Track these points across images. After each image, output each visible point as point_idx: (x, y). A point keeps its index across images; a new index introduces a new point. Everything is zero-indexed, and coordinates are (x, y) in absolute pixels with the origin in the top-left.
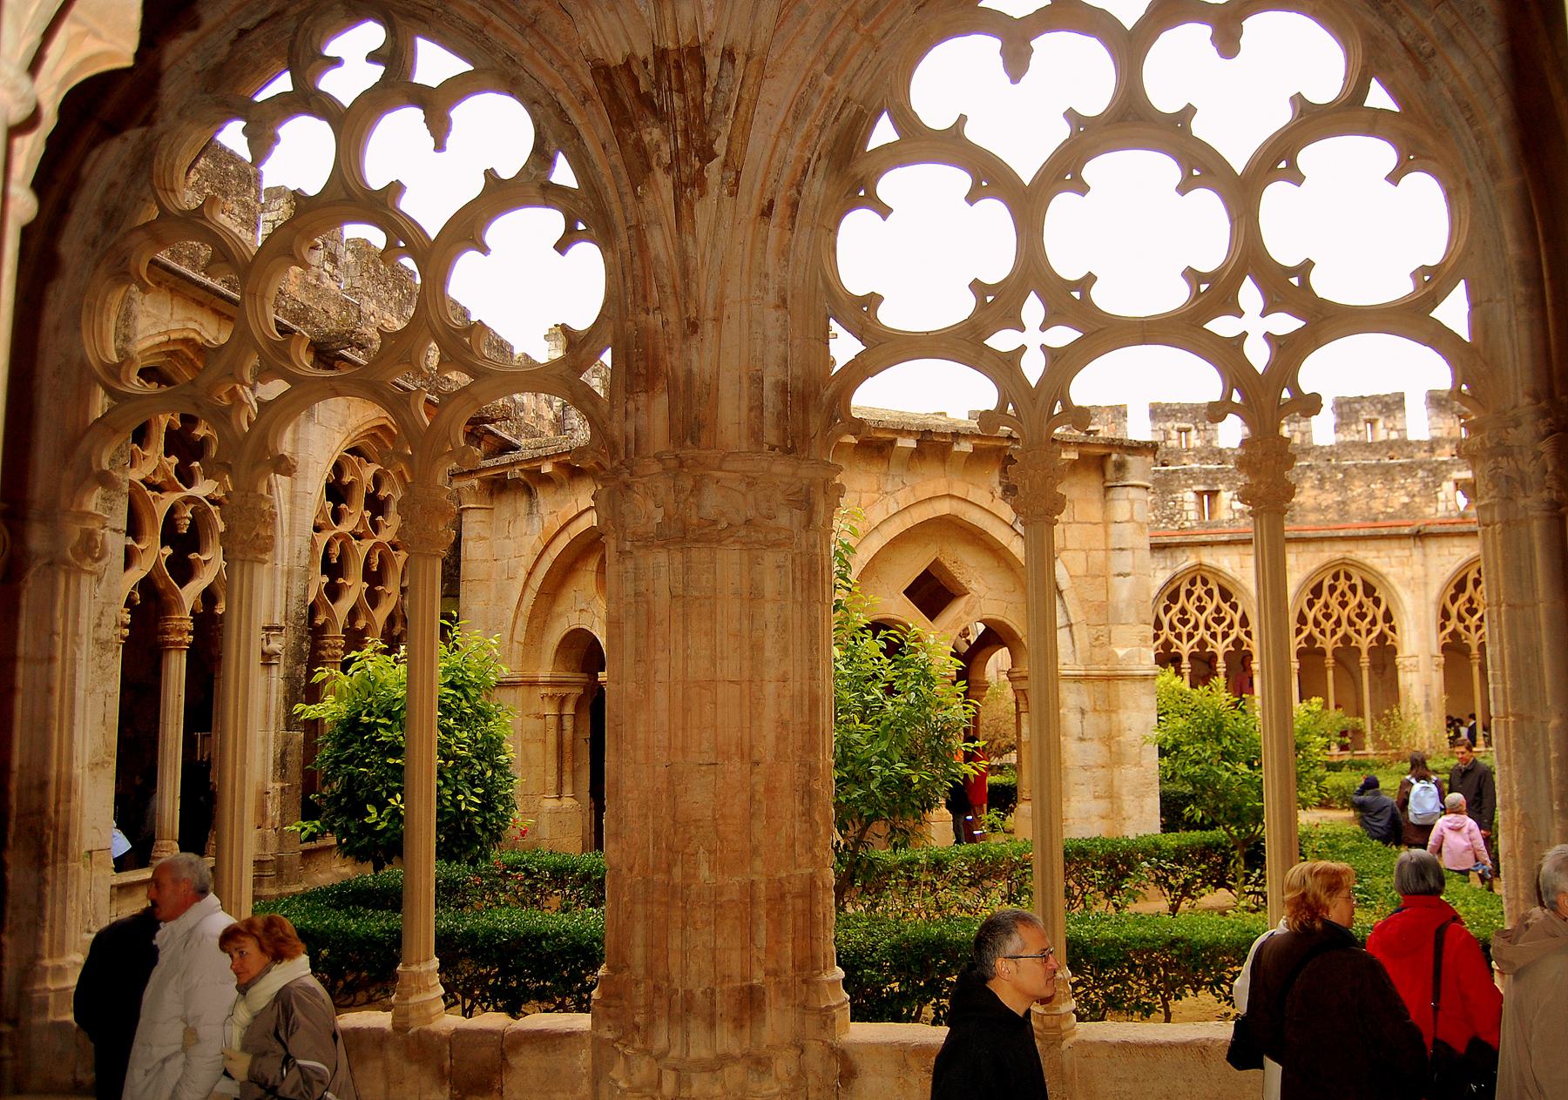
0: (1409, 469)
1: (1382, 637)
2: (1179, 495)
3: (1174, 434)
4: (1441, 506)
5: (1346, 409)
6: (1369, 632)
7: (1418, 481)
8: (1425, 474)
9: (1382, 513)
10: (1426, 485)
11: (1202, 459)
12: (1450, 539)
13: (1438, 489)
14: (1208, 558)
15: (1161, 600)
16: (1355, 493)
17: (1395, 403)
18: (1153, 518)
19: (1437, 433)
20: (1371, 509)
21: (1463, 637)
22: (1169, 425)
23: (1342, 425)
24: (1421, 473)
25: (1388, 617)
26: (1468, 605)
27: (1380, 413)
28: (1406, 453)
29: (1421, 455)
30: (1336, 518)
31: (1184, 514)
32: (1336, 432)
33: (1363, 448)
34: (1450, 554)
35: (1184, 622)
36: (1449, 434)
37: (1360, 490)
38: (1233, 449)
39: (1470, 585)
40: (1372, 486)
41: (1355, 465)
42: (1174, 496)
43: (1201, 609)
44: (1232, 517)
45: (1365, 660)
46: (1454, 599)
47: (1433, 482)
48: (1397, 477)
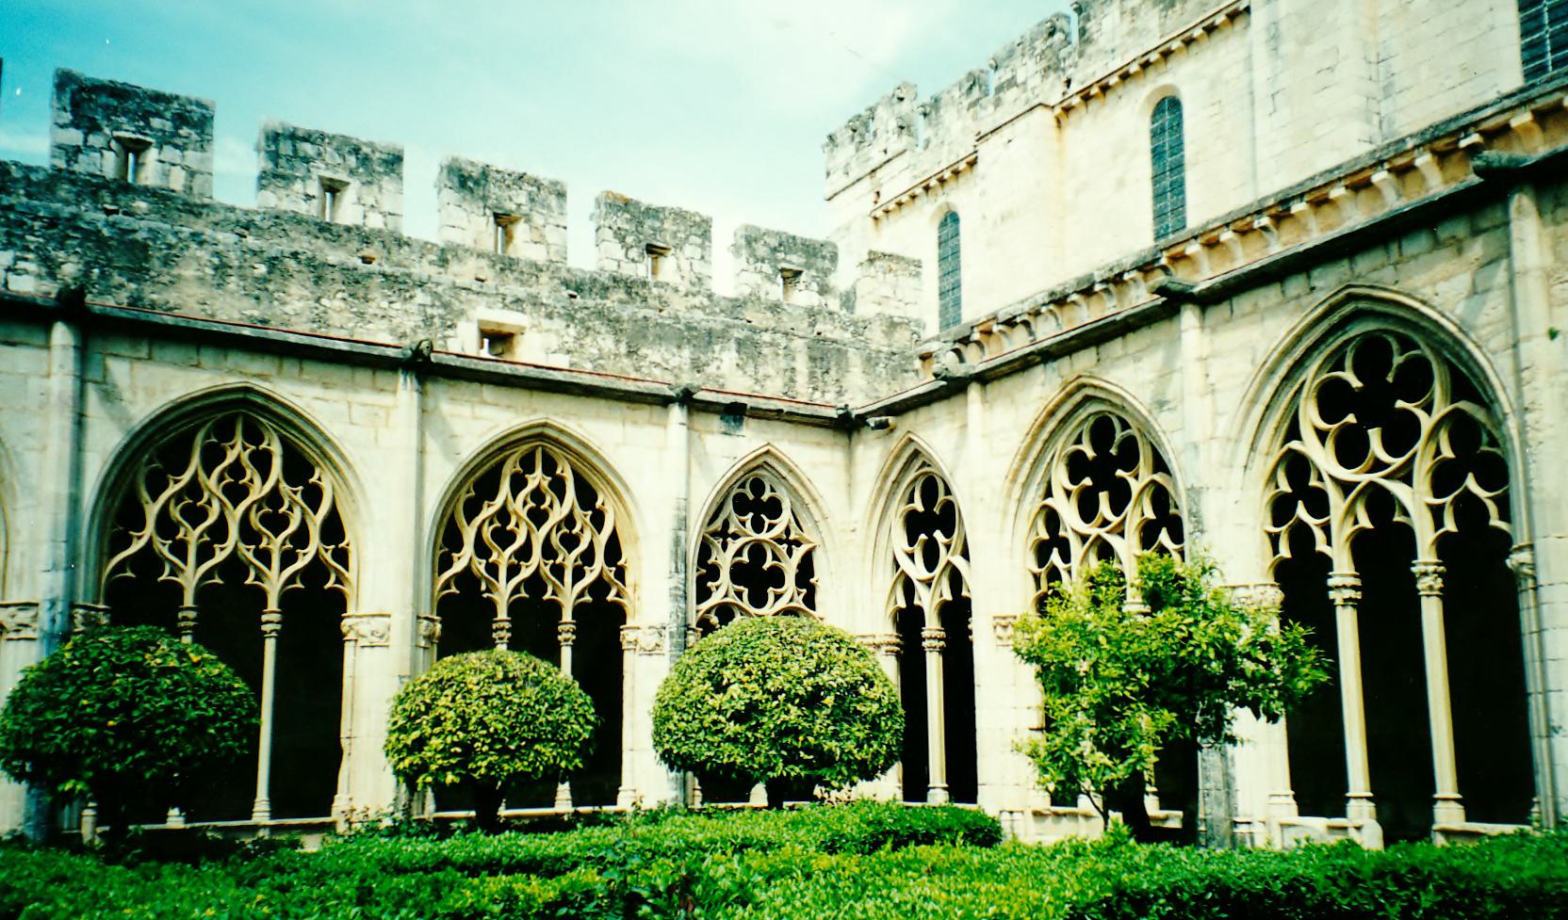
1: (317, 570)
5: (286, 148)
6: (288, 559)
8: (428, 300)
12: (476, 386)
13: (449, 332)
16: (288, 309)
19: (456, 237)
21: (483, 587)
23: (276, 176)
24: (421, 297)
25: (333, 530)
26: (497, 524)
28: (395, 258)
29: (423, 269)
32: (262, 187)
33: (314, 230)
36: (475, 241)
37: (299, 305)
38: (29, 169)
40: (324, 301)
41: (295, 255)
45: (271, 617)
46: (472, 510)
47: (441, 317)
48: (375, 294)
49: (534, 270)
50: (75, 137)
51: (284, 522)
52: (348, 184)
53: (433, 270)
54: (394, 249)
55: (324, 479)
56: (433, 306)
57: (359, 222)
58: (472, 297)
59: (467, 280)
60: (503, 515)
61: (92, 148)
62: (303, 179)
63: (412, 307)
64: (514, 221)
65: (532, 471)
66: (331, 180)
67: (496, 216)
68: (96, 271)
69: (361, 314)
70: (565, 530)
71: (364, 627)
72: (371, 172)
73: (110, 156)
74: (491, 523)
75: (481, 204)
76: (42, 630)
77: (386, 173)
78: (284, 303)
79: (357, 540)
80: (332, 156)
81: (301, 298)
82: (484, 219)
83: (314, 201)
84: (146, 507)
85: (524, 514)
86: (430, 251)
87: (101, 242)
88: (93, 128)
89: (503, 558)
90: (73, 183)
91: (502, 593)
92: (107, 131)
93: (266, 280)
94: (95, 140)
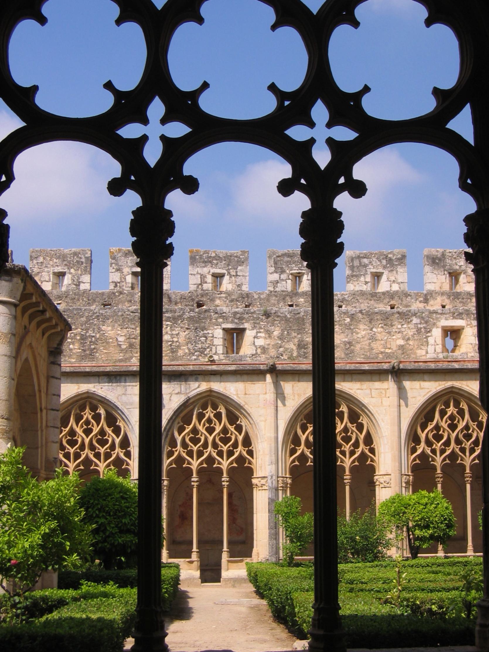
0: (405, 316)
1: (363, 457)
2: (210, 332)
3: (209, 279)
4: (431, 349)
5: (356, 263)
6: (352, 453)
7: (412, 326)
9: (382, 353)
10: (419, 331)
11: (232, 301)
13: (429, 334)
14: (218, 386)
15: (176, 422)
16: (359, 336)
17: (399, 259)
18: (187, 351)
20: (372, 349)
21: (430, 459)
22: (205, 270)
23: (352, 276)
24: (415, 320)
25: (369, 440)
26: (435, 432)
27: (385, 267)
28: (404, 303)
29: (416, 306)
30: (343, 356)
31: (214, 348)
33: (369, 297)
34: (421, 388)
35: (195, 441)
36: (441, 288)
39: (437, 416)
40: (374, 329)
41: (361, 312)
42: (205, 332)
43: (210, 430)
44: (254, 352)
49: (469, 296)
50: (275, 277)
51: (350, 438)
52: (383, 273)
53: (421, 305)
54: (404, 298)
55: (364, 420)
56: (421, 323)
57: (388, 289)
58: (438, 316)
59: (438, 308)
60: (437, 427)
61: (283, 280)
62: (364, 275)
63: (411, 326)
64: (459, 274)
65: (449, 407)
66: (376, 272)
67: (450, 273)
68: (286, 332)
69: (389, 333)
70: (465, 432)
71: (382, 479)
72: (392, 265)
73: (289, 282)
74: (432, 432)
75: (442, 270)
76: (269, 486)
77: (399, 265)
78: (357, 333)
79: (377, 444)
80: (376, 262)
81: (364, 330)
82: (444, 277)
83: (369, 284)
84: (301, 438)
85: (445, 426)
86: (420, 296)
87: (287, 320)
88: (283, 272)
89: (438, 446)
90: (276, 296)
91: (438, 461)
92: (288, 272)
93: (350, 325)
94: (284, 276)
